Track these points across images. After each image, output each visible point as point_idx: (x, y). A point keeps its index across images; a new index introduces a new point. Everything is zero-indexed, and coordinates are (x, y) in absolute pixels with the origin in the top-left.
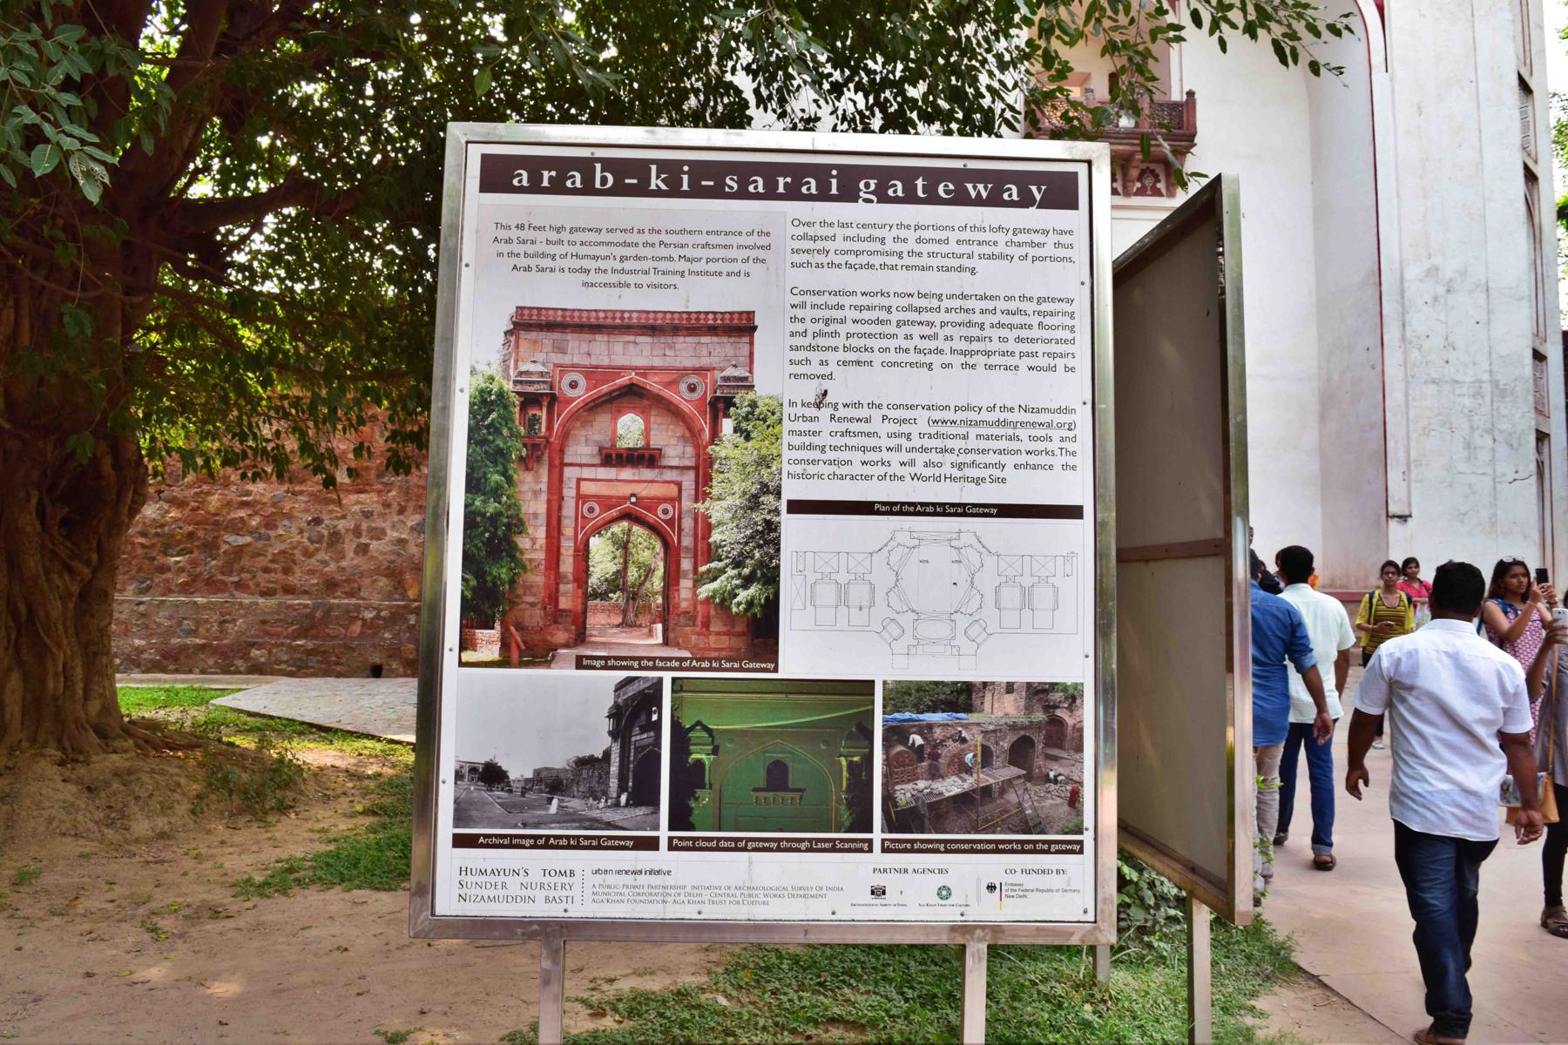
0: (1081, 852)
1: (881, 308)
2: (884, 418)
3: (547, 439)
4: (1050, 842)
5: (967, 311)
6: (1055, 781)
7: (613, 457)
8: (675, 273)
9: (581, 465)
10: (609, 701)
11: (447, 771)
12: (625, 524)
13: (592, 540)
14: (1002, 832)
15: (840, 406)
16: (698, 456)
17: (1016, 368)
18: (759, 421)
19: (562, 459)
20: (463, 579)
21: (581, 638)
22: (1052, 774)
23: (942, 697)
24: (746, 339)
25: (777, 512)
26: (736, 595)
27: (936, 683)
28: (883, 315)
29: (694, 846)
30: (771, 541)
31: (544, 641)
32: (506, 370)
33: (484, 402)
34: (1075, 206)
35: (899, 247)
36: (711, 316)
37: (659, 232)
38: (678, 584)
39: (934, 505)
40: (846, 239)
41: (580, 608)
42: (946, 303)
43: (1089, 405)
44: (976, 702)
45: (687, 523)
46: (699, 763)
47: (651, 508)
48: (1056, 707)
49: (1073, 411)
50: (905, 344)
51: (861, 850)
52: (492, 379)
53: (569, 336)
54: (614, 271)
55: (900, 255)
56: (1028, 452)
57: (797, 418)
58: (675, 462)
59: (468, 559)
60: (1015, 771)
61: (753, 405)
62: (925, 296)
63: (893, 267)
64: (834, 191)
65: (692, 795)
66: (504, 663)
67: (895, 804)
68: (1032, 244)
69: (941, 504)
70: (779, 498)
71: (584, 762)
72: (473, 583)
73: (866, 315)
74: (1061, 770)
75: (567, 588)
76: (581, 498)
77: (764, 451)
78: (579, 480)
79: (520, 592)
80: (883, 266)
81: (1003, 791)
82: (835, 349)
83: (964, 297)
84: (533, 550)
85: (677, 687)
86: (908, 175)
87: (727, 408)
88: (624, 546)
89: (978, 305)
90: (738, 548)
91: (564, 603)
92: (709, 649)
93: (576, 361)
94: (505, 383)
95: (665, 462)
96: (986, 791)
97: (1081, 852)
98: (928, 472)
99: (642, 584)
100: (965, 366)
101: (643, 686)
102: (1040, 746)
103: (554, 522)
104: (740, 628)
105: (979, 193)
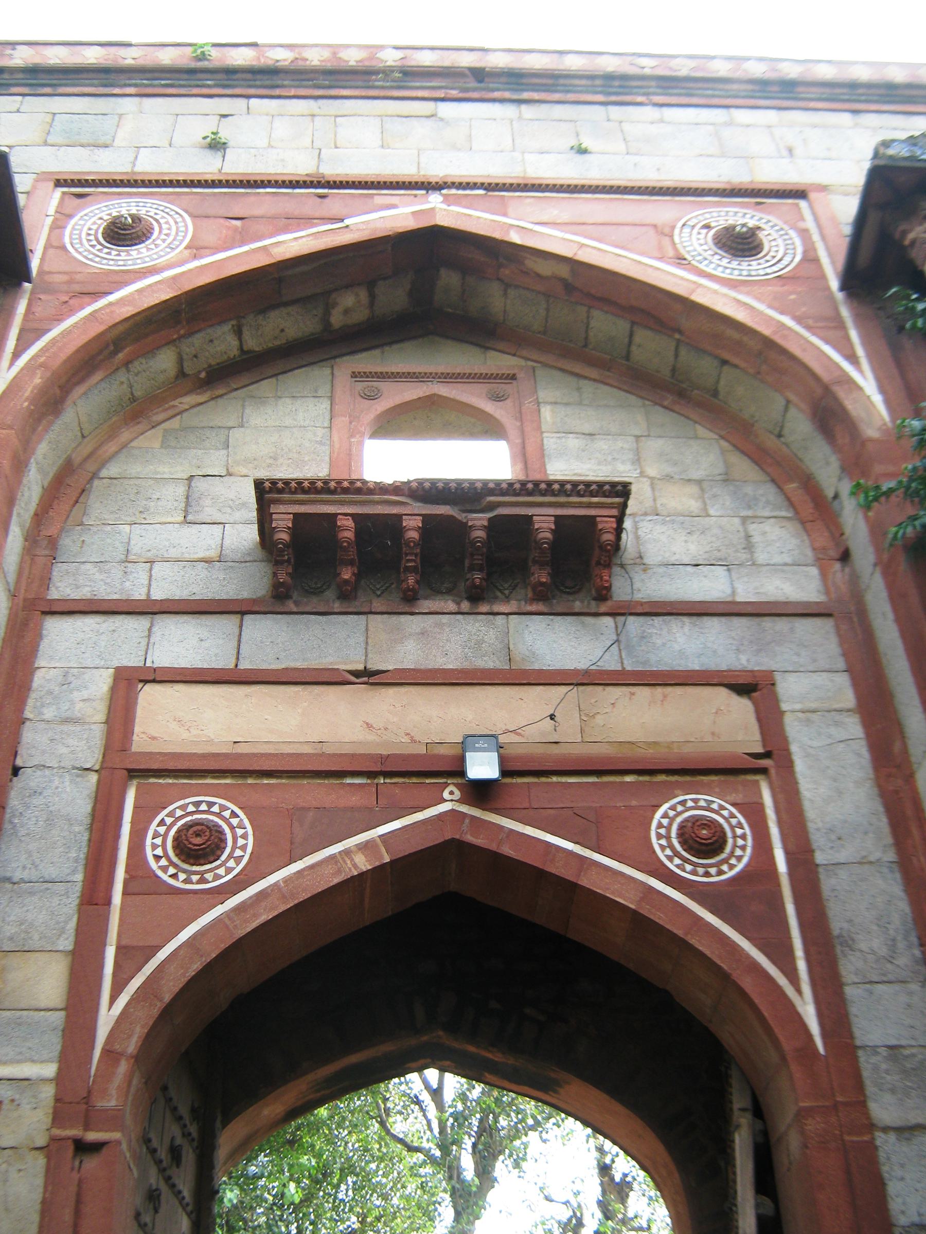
53: (128, 105)
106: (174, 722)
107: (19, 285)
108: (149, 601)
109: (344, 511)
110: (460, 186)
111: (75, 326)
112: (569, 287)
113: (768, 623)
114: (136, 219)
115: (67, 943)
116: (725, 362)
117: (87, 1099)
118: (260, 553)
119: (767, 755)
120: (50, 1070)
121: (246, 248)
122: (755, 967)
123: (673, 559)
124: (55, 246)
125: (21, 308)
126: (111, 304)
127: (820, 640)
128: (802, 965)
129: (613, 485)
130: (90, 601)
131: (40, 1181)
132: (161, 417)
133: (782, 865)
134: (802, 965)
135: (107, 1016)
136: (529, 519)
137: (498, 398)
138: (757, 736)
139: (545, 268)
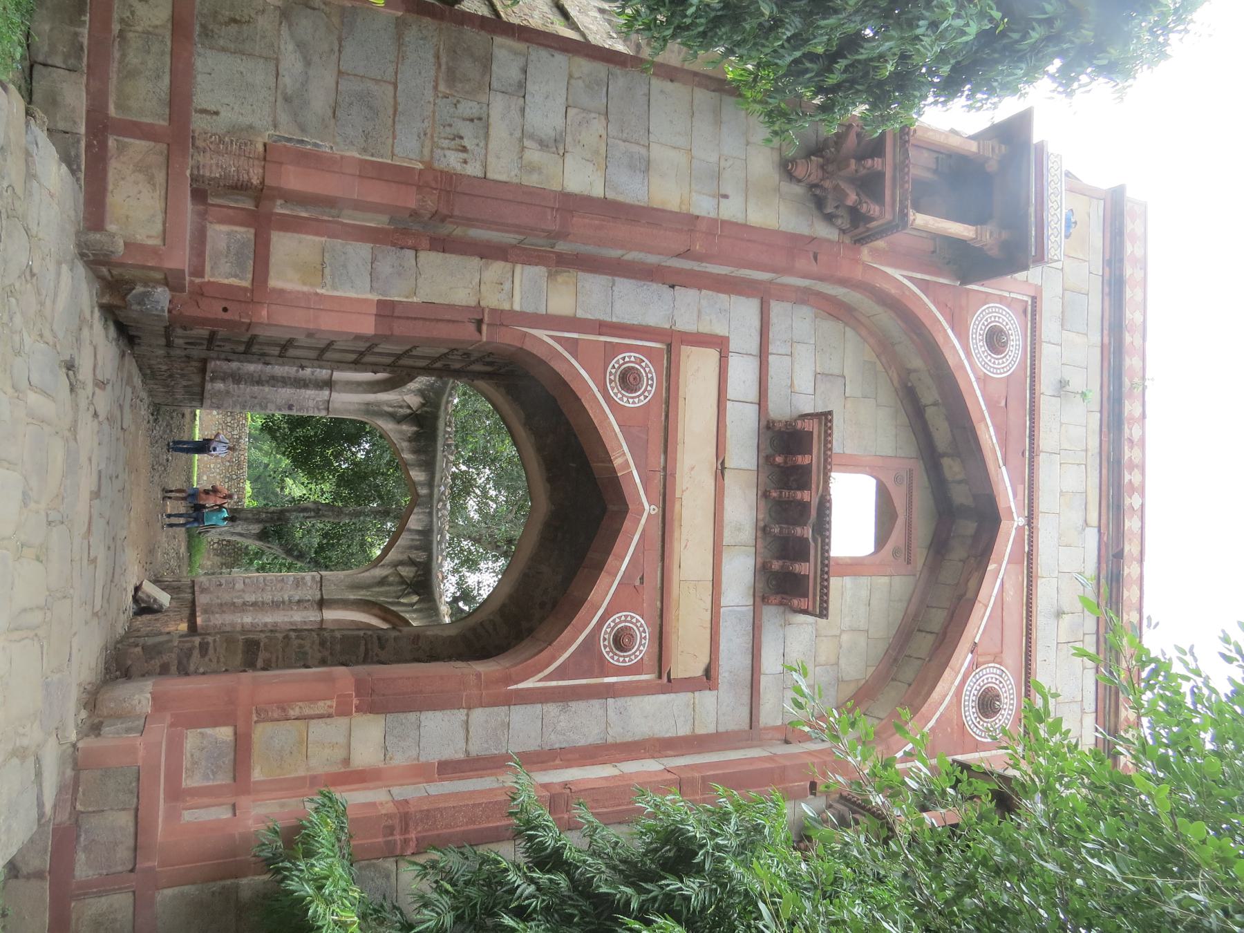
19: (784, 294)
76: (671, 344)
78: (720, 344)
84: (524, 135)
93: (1048, 353)
106: (698, 368)
107: (958, 279)
108: (768, 354)
109: (812, 459)
110: (1031, 536)
111: (931, 311)
112: (960, 597)
113: (748, 691)
114: (1005, 345)
115: (580, 314)
116: (910, 685)
117: (502, 325)
118: (795, 415)
119: (669, 680)
120: (517, 307)
121: (984, 408)
122: (554, 659)
123: (788, 642)
124: (987, 298)
125: (942, 280)
126: (945, 331)
127: (736, 719)
128: (554, 683)
129: (827, 609)
130: (768, 322)
131: (464, 303)
132: (884, 360)
133: (607, 680)
134: (554, 683)
135: (542, 334)
136: (808, 561)
137: (895, 553)
138: (680, 676)
139: (972, 584)
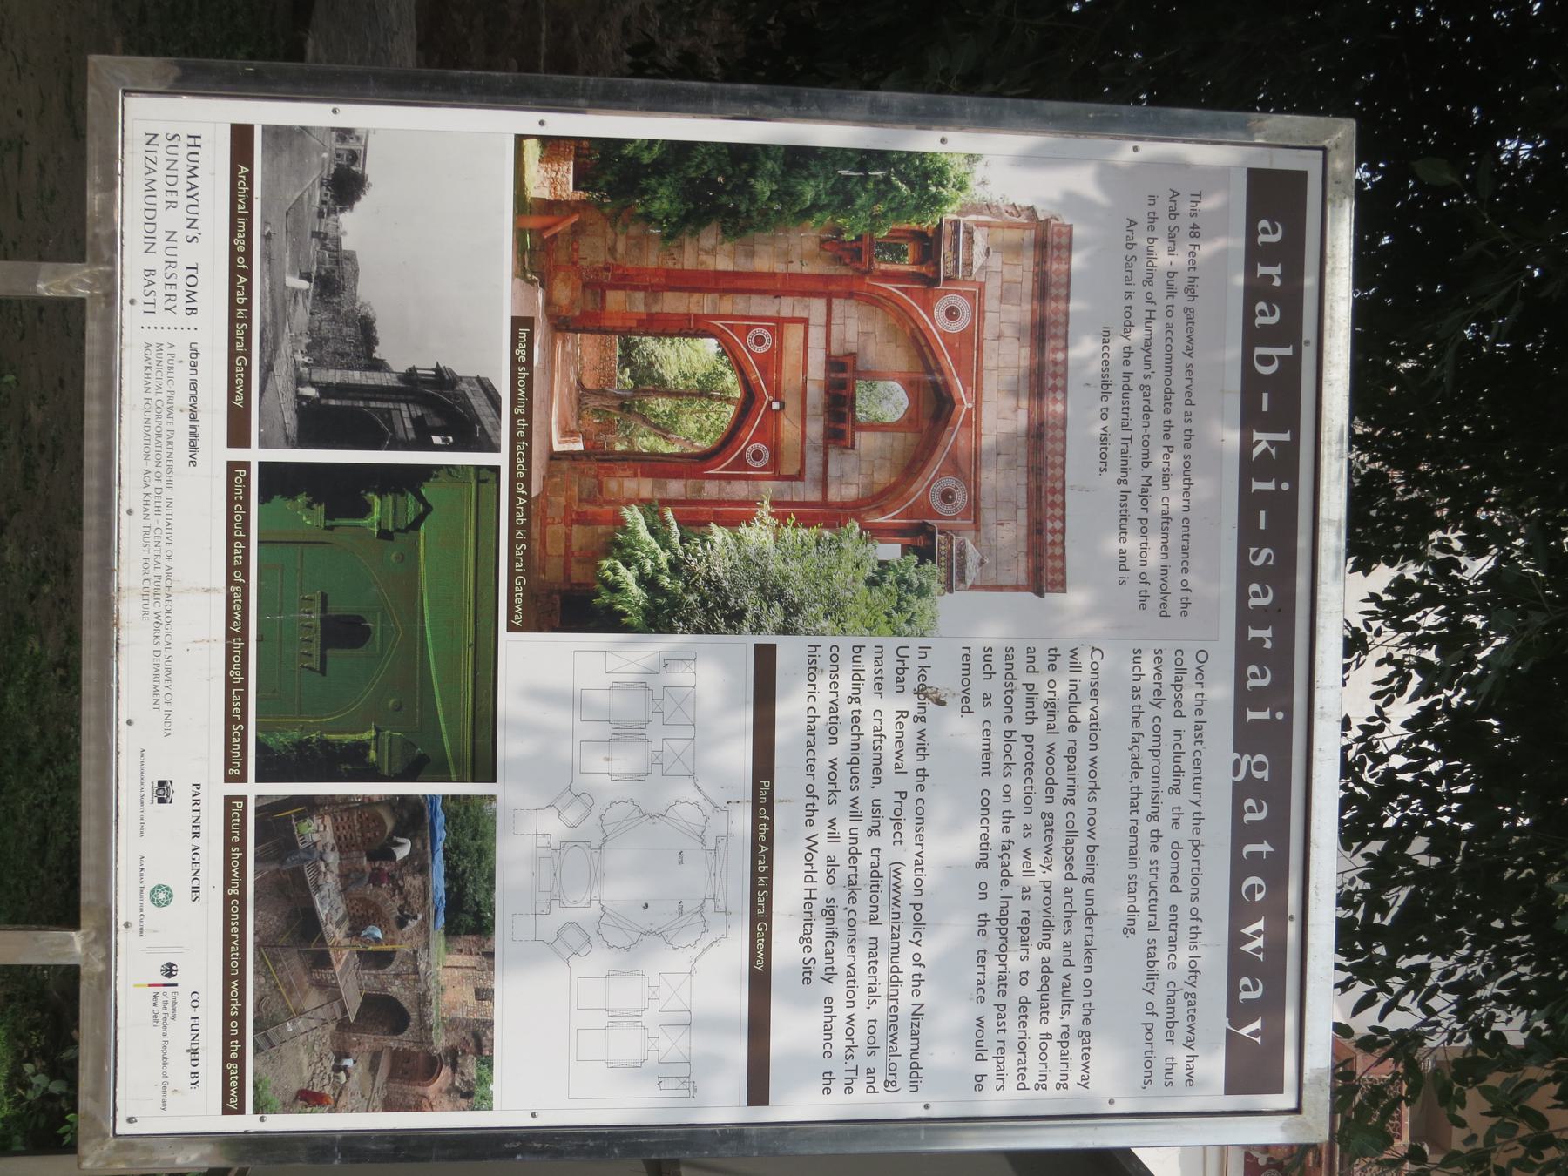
0: (226, 1111)
1: (1072, 788)
2: (903, 794)
3: (869, 272)
4: (241, 1061)
5: (1068, 922)
6: (337, 1069)
7: (843, 379)
8: (1124, 469)
9: (828, 324)
10: (463, 367)
11: (353, 115)
12: (738, 393)
13: (713, 342)
14: (257, 986)
15: (920, 726)
16: (843, 505)
17: (981, 999)
18: (897, 602)
19: (838, 297)
20: (652, 142)
21: (561, 324)
22: (349, 1063)
23: (470, 888)
24: (1023, 579)
25: (757, 628)
26: (627, 565)
27: (491, 879)
28: (1061, 792)
29: (235, 502)
30: (712, 620)
31: (557, 268)
32: (976, 209)
33: (927, 175)
34: (1231, 1088)
35: (1166, 816)
36: (1058, 525)
37: (1187, 445)
38: (645, 475)
39: (769, 873)
40: (1178, 733)
41: (608, 323)
42: (1079, 889)
43: (923, 1114)
44: (463, 941)
45: (740, 490)
46: (366, 510)
47: (760, 435)
48: (454, 1066)
49: (915, 1089)
50: (1016, 826)
51: (228, 763)
52: (962, 187)
53: (1027, 307)
54: (1127, 375)
55: (1153, 817)
56: (850, 1019)
57: (902, 659)
58: (833, 470)
59: (681, 150)
60: (354, 1005)
61: (922, 592)
62: (1091, 856)
63: (1134, 807)
64: (1252, 715)
65: (316, 498)
66: (522, 205)
67: (301, 817)
68: (1172, 1022)
69: (770, 882)
70: (778, 632)
71: (366, 331)
72: (647, 158)
73: (1061, 765)
74: (355, 1077)
75: (638, 303)
76: (778, 325)
77: (850, 608)
79: (634, 230)
80: (1136, 792)
81: (322, 985)
82: (1009, 718)
83: (1090, 916)
85: (484, 474)
86: (1276, 829)
87: (917, 551)
88: (704, 392)
89: (1077, 939)
90: (702, 569)
91: (615, 300)
92: (544, 525)
93: (990, 318)
94: (955, 207)
95: (833, 454)
96: (322, 960)
97: (226, 1111)
98: (820, 863)
99: (645, 420)
100: (984, 919)
101: (487, 421)
102: (393, 1042)
103: (740, 284)
104: (578, 573)
105: (1249, 939)
124: (946, 292)
135: (718, 323)
